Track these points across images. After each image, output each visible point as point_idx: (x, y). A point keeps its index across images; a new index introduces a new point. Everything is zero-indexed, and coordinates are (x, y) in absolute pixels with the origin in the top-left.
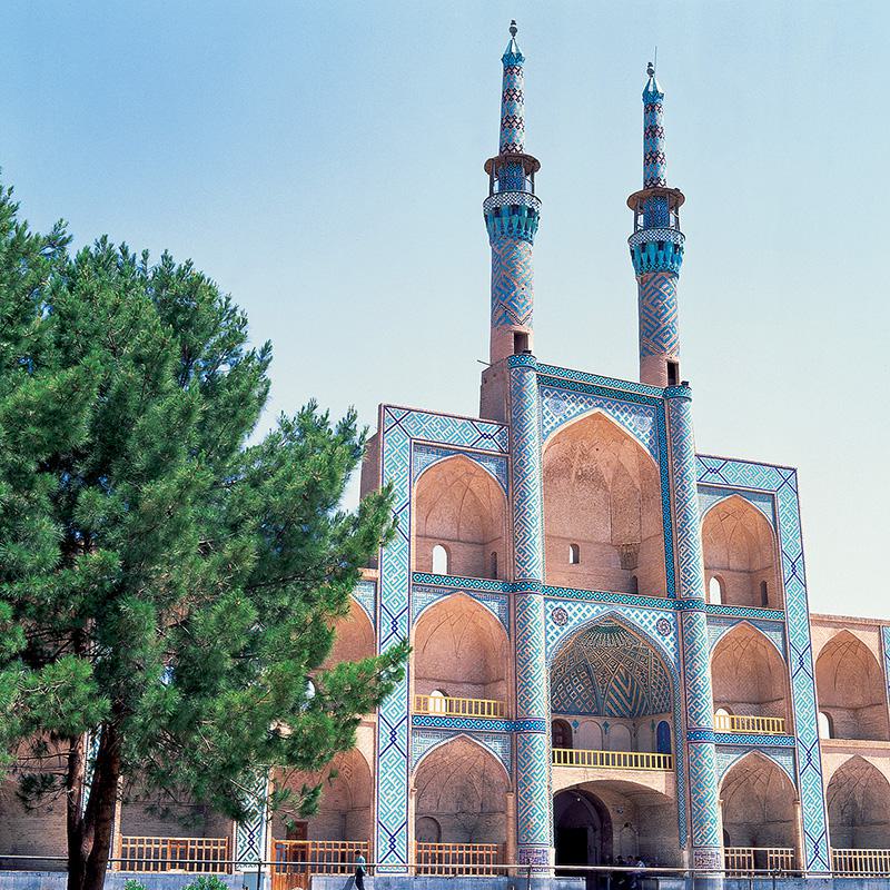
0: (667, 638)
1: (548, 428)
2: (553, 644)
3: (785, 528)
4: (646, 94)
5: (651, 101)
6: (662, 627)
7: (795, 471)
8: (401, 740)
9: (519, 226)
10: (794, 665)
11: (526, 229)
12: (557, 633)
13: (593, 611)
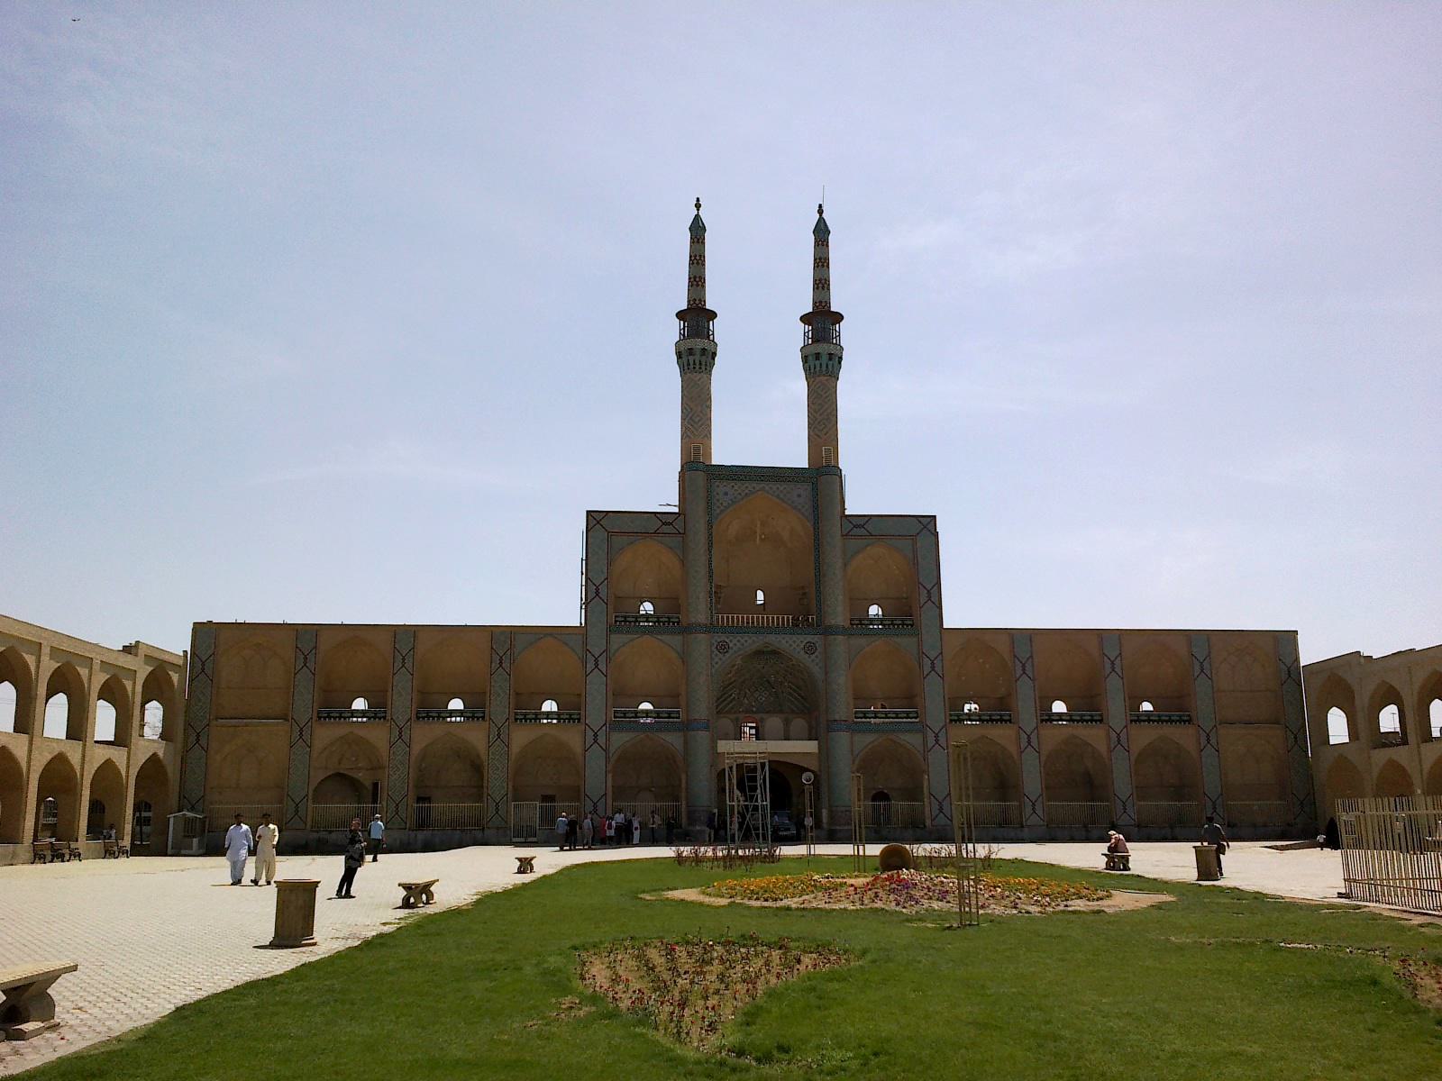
0: (813, 656)
1: (718, 511)
2: (717, 666)
5: (821, 233)
6: (810, 649)
8: (602, 740)
10: (927, 669)
11: (706, 365)
12: (720, 659)
13: (750, 641)
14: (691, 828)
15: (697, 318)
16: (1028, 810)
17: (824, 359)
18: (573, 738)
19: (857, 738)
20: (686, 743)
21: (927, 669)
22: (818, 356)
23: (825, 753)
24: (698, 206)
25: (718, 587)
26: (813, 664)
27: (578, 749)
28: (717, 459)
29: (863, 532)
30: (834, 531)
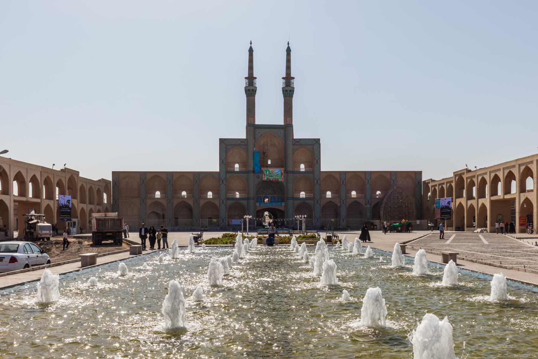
4: (287, 51)
7: (319, 139)
8: (224, 203)
16: (342, 221)
17: (289, 91)
18: (217, 202)
20: (248, 203)
21: (316, 182)
22: (286, 91)
23: (286, 206)
27: (218, 205)
29: (298, 143)
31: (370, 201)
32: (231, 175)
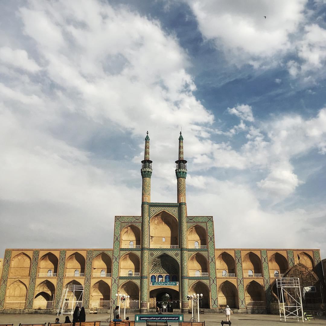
1: (151, 216)
3: (209, 230)
5: (181, 139)
6: (177, 255)
7: (212, 217)
9: (146, 175)
10: (210, 261)
12: (151, 258)
14: (142, 308)
15: (147, 162)
18: (108, 281)
19: (190, 281)
20: (141, 283)
22: (179, 172)
23: (182, 286)
24: (147, 133)
25: (152, 237)
26: (178, 259)
27: (110, 285)
28: (151, 202)
30: (184, 220)
31: (268, 281)
32: (124, 252)
